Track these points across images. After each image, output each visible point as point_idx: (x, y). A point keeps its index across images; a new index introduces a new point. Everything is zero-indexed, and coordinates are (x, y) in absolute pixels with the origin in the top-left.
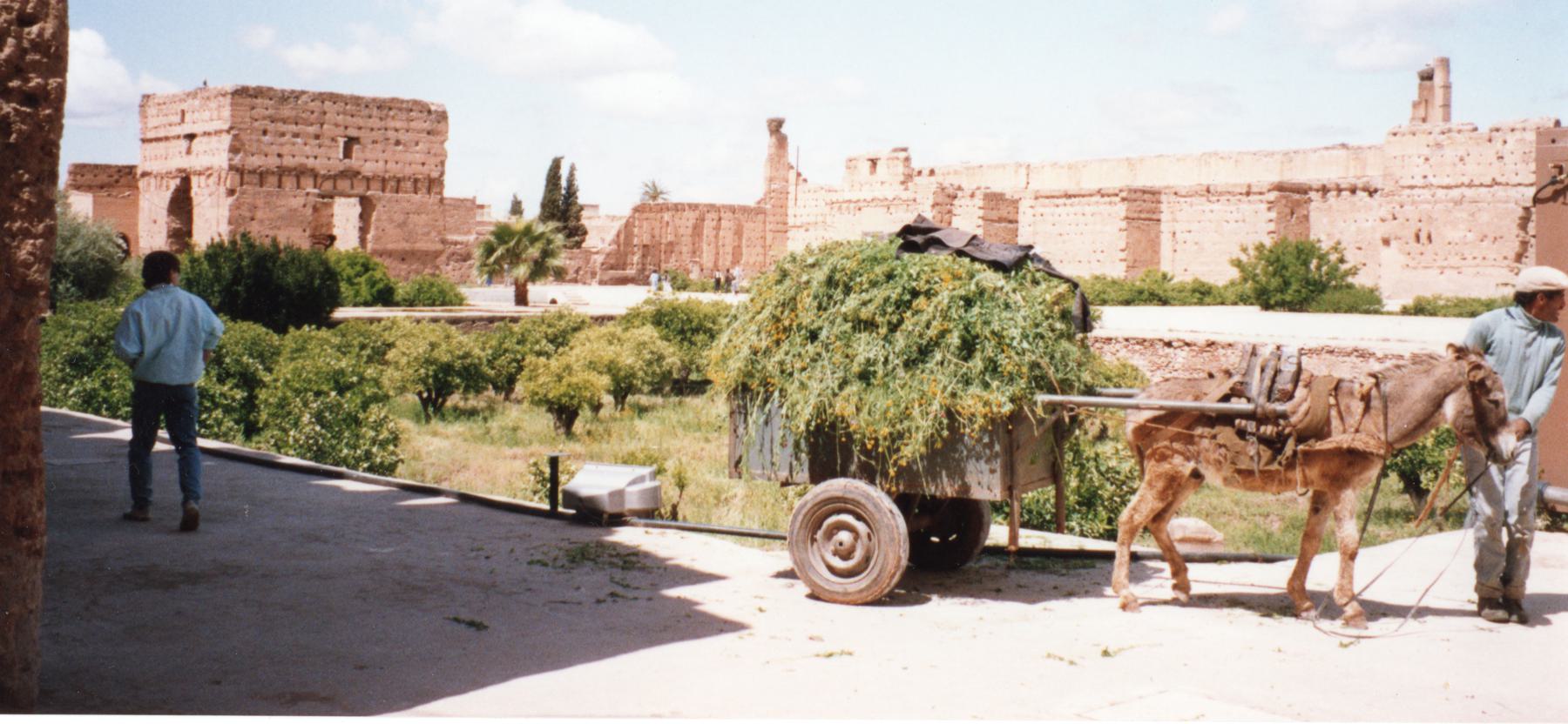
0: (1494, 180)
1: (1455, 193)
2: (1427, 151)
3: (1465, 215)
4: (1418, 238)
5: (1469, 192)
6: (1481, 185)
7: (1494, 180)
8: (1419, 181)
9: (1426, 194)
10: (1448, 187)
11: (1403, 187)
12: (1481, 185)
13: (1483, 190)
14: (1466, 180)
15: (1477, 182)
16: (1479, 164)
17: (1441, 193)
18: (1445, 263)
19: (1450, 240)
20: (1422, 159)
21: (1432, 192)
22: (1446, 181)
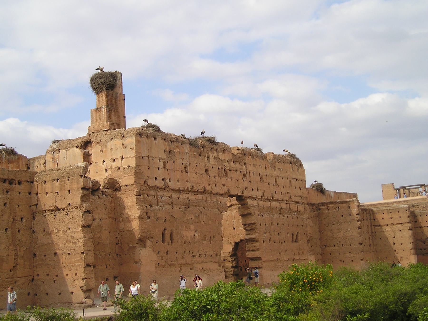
2: (164, 156)
4: (163, 241)
5: (192, 197)
6: (198, 192)
8: (161, 184)
9: (167, 194)
10: (179, 191)
12: (198, 192)
13: (200, 197)
14: (189, 185)
15: (195, 189)
17: (175, 195)
18: (183, 262)
20: (161, 164)
21: (169, 194)
22: (178, 185)
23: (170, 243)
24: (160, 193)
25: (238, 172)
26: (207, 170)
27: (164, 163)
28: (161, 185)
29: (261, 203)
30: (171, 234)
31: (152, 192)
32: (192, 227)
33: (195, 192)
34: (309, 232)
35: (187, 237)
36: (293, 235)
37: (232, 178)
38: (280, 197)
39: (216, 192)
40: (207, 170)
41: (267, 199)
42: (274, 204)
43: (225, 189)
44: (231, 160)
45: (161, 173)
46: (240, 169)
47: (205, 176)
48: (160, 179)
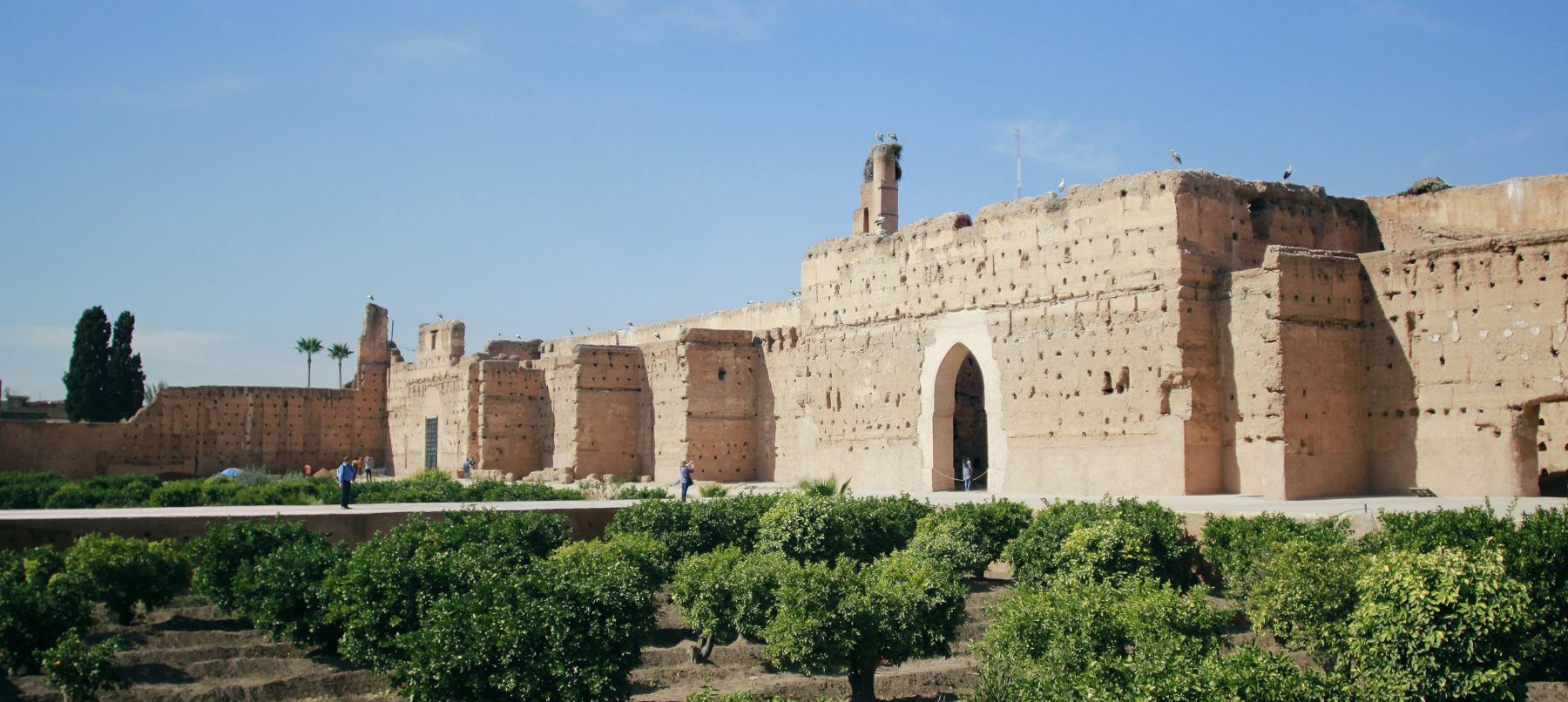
0: (898, 311)
1: (863, 331)
3: (869, 364)
5: (875, 331)
7: (898, 311)
8: (830, 321)
11: (817, 329)
12: (887, 320)
13: (889, 327)
16: (883, 289)
17: (850, 334)
19: (856, 400)
23: (836, 409)
24: (830, 334)
25: (969, 262)
26: (904, 279)
27: (837, 287)
28: (832, 323)
29: (1018, 315)
30: (839, 394)
31: (819, 336)
32: (868, 381)
33: (882, 321)
34: (1164, 363)
35: (859, 397)
36: (1107, 374)
37: (951, 278)
38: (1077, 288)
39: (917, 312)
40: (904, 279)
41: (1039, 301)
42: (1057, 309)
43: (938, 304)
44: (951, 244)
45: (834, 304)
46: (972, 254)
47: (900, 288)
48: (830, 313)
